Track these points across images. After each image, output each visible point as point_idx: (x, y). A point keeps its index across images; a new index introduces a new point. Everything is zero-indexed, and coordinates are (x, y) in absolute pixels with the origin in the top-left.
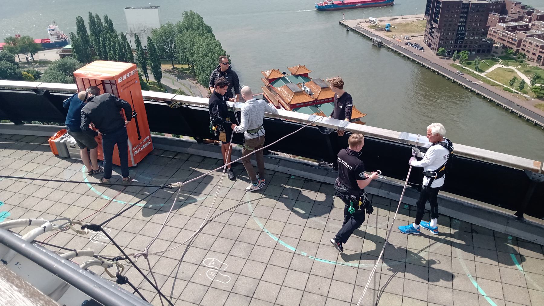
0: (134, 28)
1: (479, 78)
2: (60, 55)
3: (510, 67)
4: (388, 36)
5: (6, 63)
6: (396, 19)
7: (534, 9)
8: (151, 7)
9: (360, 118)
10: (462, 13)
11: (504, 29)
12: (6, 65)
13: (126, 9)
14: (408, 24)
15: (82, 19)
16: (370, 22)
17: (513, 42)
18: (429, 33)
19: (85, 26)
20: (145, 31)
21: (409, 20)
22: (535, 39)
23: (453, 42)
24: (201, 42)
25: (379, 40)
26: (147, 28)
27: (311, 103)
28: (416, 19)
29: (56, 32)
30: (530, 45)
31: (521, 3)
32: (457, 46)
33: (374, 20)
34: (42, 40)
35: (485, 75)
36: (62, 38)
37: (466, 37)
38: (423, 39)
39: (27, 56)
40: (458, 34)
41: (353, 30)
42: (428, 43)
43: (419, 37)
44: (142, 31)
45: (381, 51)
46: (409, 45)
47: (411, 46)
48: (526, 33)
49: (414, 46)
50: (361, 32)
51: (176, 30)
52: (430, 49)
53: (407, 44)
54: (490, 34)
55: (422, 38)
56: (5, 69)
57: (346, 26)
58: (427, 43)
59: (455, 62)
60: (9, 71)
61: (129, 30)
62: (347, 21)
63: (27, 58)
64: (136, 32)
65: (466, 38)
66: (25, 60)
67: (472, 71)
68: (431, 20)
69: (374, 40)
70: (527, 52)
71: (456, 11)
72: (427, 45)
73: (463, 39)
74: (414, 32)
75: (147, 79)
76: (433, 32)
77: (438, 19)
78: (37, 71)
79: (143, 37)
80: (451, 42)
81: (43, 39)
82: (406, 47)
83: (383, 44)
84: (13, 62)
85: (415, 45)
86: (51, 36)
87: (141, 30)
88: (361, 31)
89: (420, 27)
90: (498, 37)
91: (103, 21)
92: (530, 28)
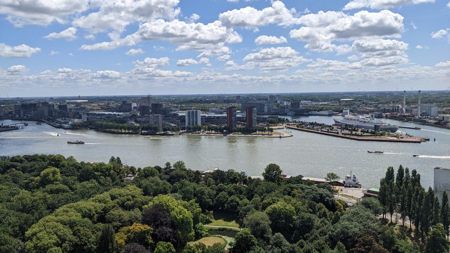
15: (393, 170)
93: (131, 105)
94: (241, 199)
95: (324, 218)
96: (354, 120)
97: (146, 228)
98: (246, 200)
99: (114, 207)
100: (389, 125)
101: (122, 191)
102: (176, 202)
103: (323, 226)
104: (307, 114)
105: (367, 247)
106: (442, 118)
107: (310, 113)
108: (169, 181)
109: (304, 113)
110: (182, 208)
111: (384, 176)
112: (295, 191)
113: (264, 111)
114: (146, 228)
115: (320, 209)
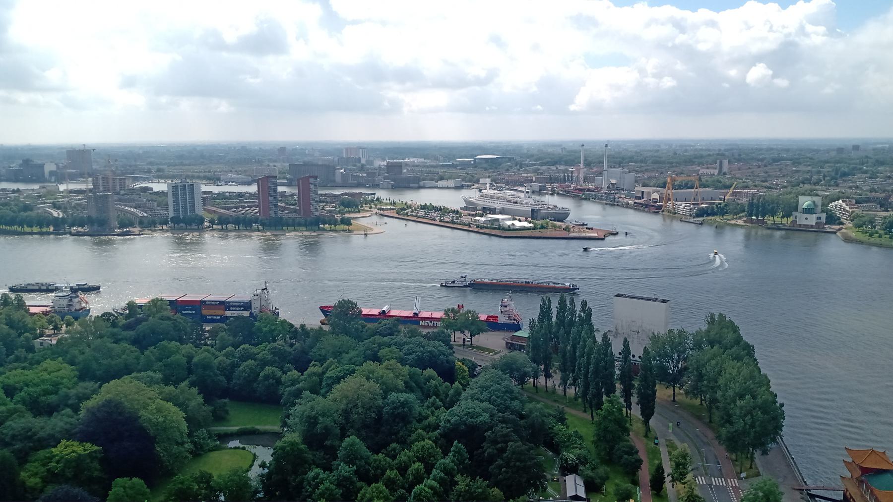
0: (622, 325)
2: (507, 343)
8: (655, 300)
12: (440, 348)
13: (616, 296)
19: (551, 310)
20: (638, 332)
24: (734, 372)
29: (509, 310)
34: (488, 317)
36: (514, 320)
39: (465, 337)
44: (634, 333)
51: (690, 343)
63: (464, 339)
66: (461, 343)
75: (629, 411)
78: (474, 362)
79: (633, 341)
81: (491, 315)
84: (447, 342)
87: (632, 330)
91: (578, 308)
93: (42, 166)
94: (285, 373)
95: (434, 397)
96: (498, 198)
97: (87, 450)
98: (295, 373)
99: (11, 413)
100: (556, 207)
101: (30, 375)
102: (152, 392)
103: (432, 413)
104: (416, 185)
106: (641, 193)
107: (422, 183)
108: (135, 342)
109: (411, 185)
110: (162, 401)
112: (384, 351)
113: (334, 181)
114: (87, 450)
115: (428, 380)
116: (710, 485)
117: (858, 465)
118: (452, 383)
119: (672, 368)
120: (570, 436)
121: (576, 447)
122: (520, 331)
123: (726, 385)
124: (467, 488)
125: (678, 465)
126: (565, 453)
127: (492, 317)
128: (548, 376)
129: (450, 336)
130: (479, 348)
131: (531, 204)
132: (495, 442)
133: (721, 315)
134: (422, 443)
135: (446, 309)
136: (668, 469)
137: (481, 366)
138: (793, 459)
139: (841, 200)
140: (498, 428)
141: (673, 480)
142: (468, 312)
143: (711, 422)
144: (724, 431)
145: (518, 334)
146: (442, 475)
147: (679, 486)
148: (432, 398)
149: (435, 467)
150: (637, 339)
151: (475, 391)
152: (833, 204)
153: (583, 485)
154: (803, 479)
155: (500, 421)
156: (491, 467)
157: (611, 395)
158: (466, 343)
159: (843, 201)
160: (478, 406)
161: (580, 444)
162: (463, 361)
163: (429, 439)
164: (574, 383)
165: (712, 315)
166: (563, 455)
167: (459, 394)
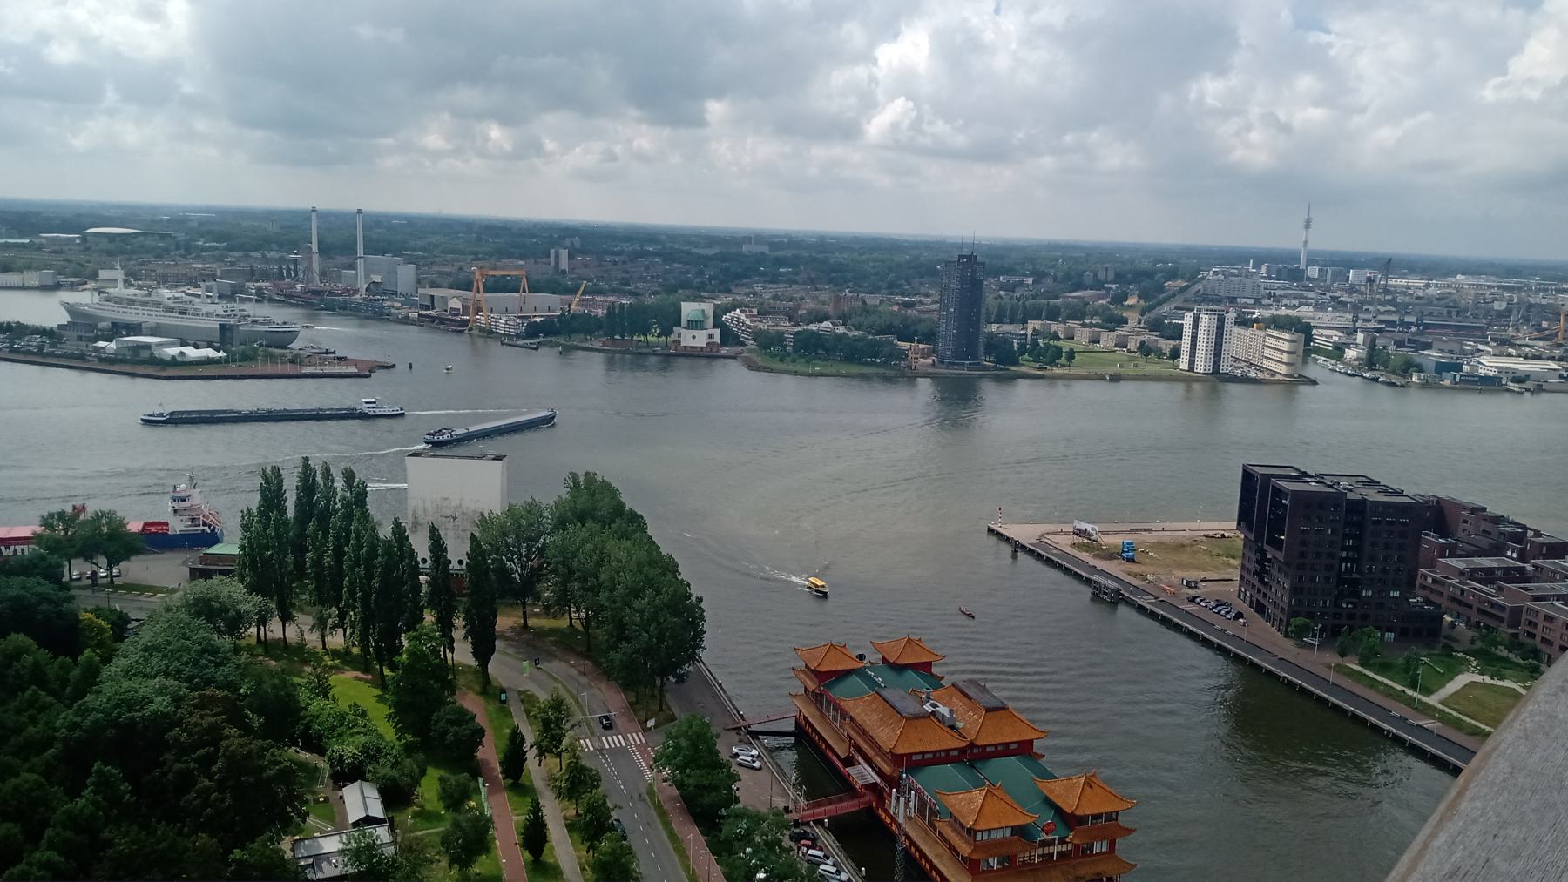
1: (1427, 710)
2: (192, 571)
3: (1507, 683)
4: (1136, 576)
5: (38, 583)
6: (1145, 530)
7: (1524, 527)
9: (1117, 812)
10: (1347, 524)
11: (1462, 573)
12: (39, 589)
14: (1183, 546)
16: (1077, 534)
17: (1498, 613)
18: (1256, 573)
20: (455, 518)
21: (1184, 537)
22: (1558, 607)
23: (1328, 602)
25: (1111, 584)
26: (463, 513)
27: (956, 753)
28: (1202, 533)
29: (192, 506)
30: (1547, 624)
31: (1486, 508)
32: (1340, 615)
33: (1089, 529)
34: (146, 525)
35: (1442, 703)
37: (1364, 592)
38: (1237, 589)
39: (95, 568)
40: (1341, 581)
41: (1031, 552)
42: (1255, 600)
43: (1223, 584)
45: (1118, 612)
46: (1199, 604)
47: (1206, 606)
48: (1526, 589)
49: (1214, 608)
50: (1054, 558)
51: (547, 521)
52: (1263, 617)
53: (1192, 600)
54: (1424, 587)
55: (1233, 587)
56: (34, 599)
57: (1008, 540)
58: (1251, 602)
59: (1345, 658)
60: (44, 607)
61: (410, 512)
62: (1007, 526)
64: (431, 519)
65: (1364, 594)
67: (1399, 688)
68: (1258, 538)
69: (1096, 582)
70: (1541, 642)
71: (1331, 518)
72: (1251, 606)
73: (1357, 595)
74: (1205, 570)
76: (1267, 572)
77: (1283, 537)
80: (1325, 603)
82: (1190, 607)
83: (1122, 595)
85: (1217, 606)
86: (175, 516)
87: (444, 515)
88: (1053, 554)
89: (1218, 555)
90: (1448, 596)
91: (339, 483)
92: (1531, 578)
96: (144, 304)
105: (201, 752)
106: (429, 298)
111: (253, 503)
116: (602, 749)
117: (812, 671)
118: (75, 653)
119: (519, 569)
120: (342, 717)
121: (358, 733)
122: (219, 545)
123: (612, 579)
124: (135, 847)
125: (546, 724)
126: (336, 747)
127: (154, 524)
128: (286, 618)
129: (62, 566)
130: (129, 588)
131: (217, 315)
132: (184, 750)
133: (587, 473)
134: (14, 781)
135: (45, 514)
136: (530, 735)
137: (137, 620)
138: (720, 684)
139: (738, 310)
140: (194, 719)
141: (541, 754)
142: (98, 517)
143: (589, 650)
144: (617, 657)
145: (216, 549)
146: (69, 834)
147: (551, 762)
148: (29, 692)
149: (52, 822)
150: (454, 529)
151: (134, 657)
152: (728, 316)
153: (376, 795)
154: (738, 712)
155: (195, 706)
156: (184, 798)
157: (418, 626)
158: (100, 581)
159: (741, 312)
160: (145, 688)
161: (365, 726)
162: (98, 612)
163: (30, 770)
164: (340, 625)
165: (574, 476)
166: (333, 751)
167: (97, 672)
